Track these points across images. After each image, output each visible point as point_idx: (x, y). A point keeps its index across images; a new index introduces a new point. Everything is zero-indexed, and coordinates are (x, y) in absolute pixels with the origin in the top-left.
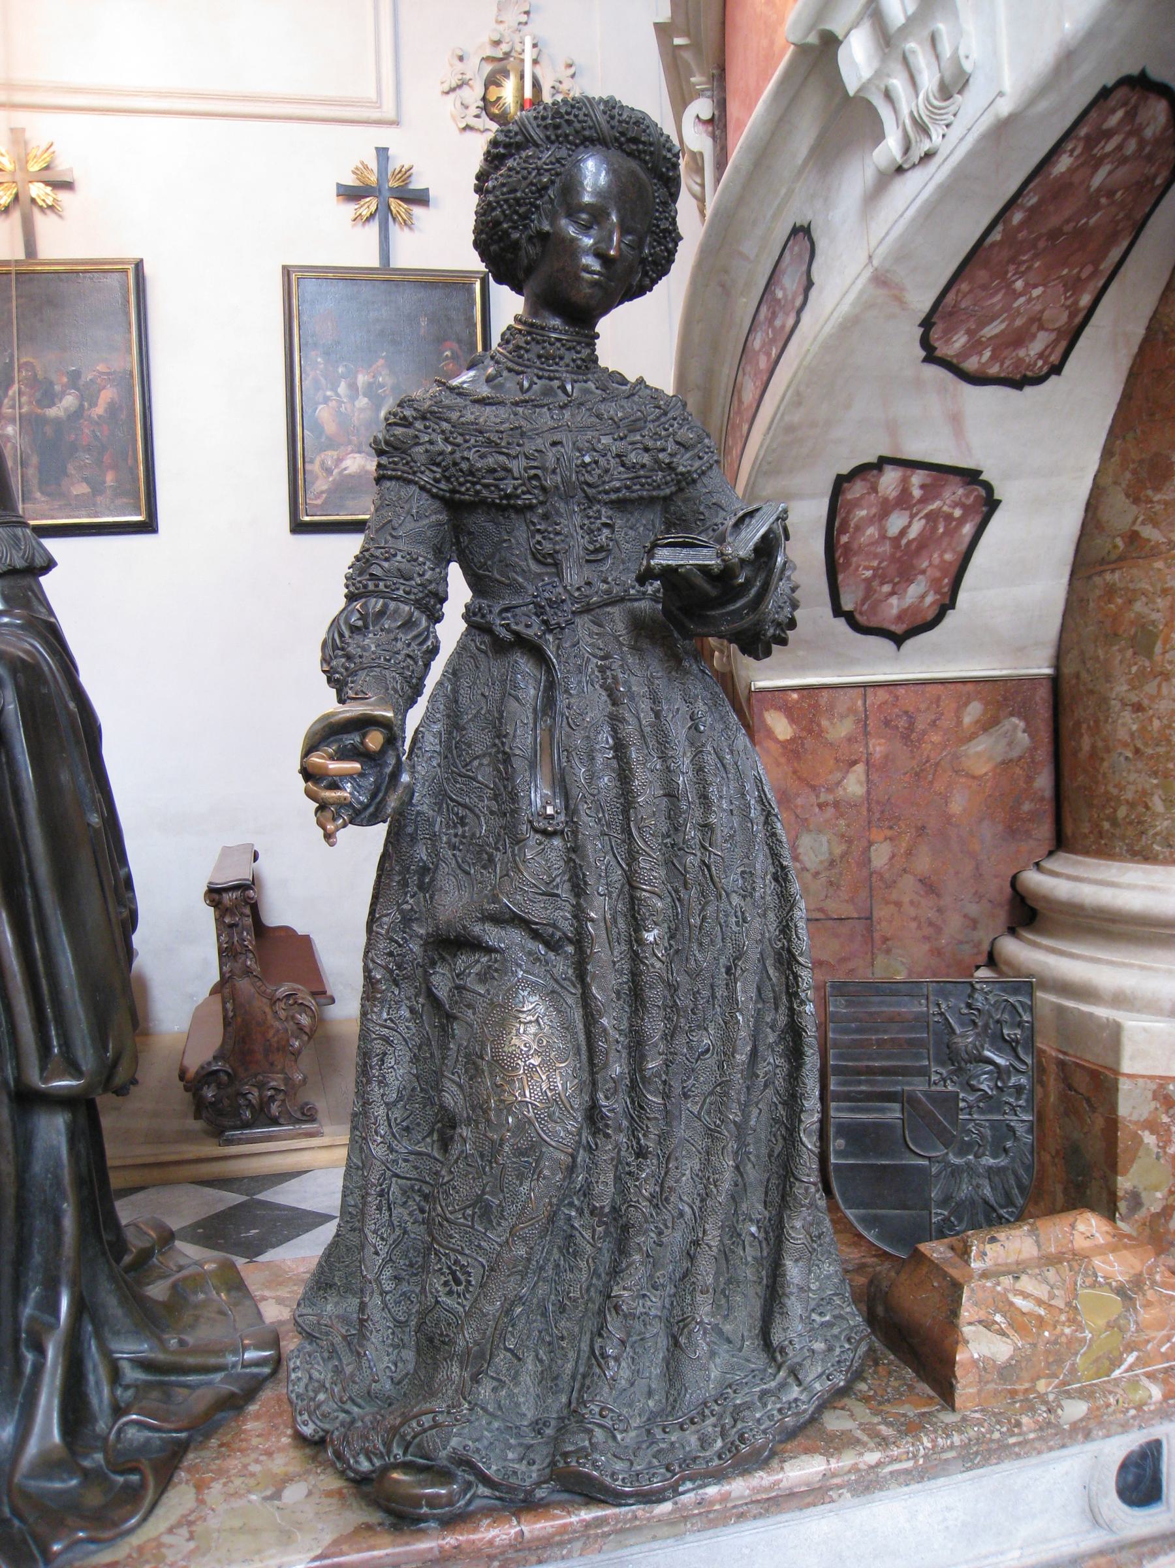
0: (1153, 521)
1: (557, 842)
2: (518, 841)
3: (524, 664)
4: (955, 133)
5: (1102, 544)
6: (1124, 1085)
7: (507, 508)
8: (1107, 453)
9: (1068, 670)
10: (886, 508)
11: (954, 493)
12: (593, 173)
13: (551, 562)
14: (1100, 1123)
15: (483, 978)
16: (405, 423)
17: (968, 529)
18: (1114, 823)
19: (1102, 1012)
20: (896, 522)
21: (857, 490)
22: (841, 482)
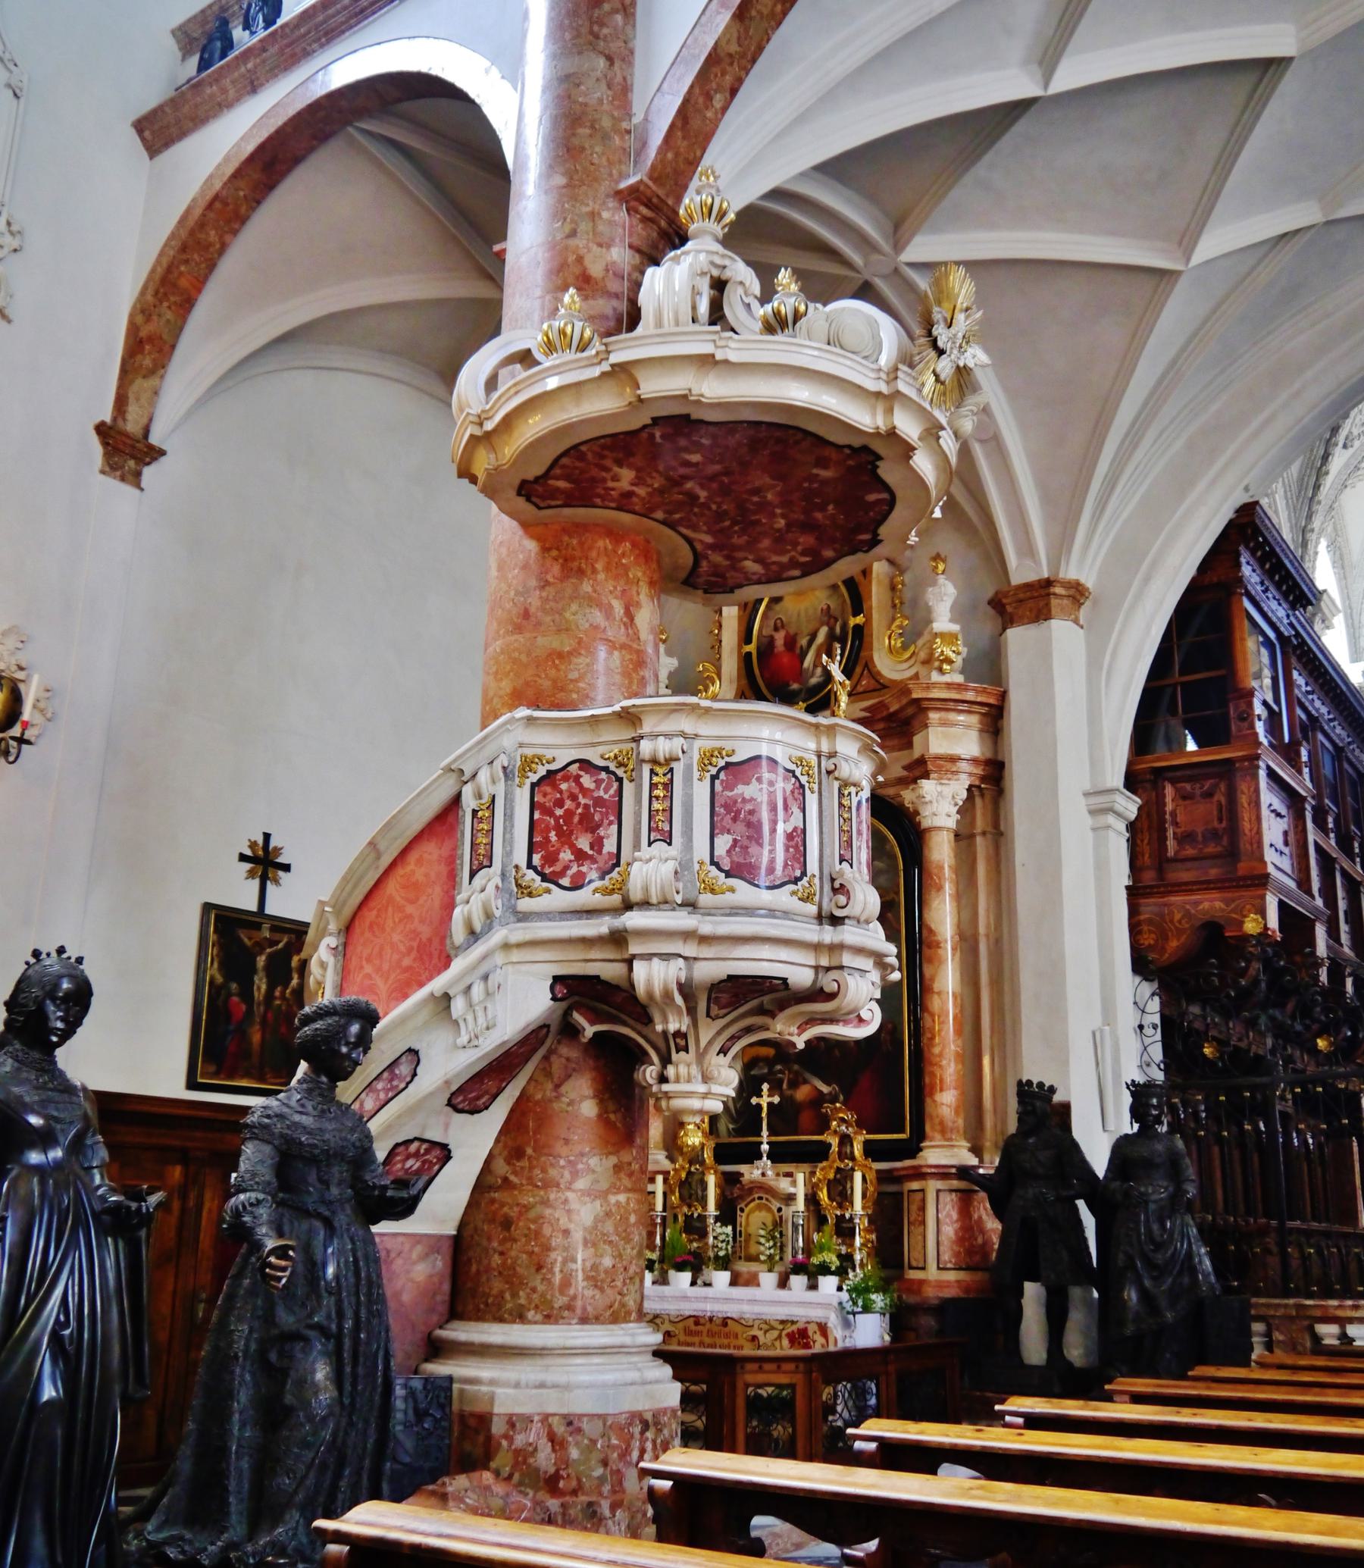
0: (515, 1173)
1: (333, 1298)
2: (319, 1297)
3: (318, 1224)
4: (488, 1042)
5: (490, 1180)
6: (495, 1419)
7: (313, 1161)
8: (497, 1141)
9: (466, 1234)
10: (408, 1157)
11: (437, 1152)
12: (355, 1028)
13: (326, 1184)
14: (481, 1439)
15: (303, 1350)
16: (268, 1117)
17: (436, 1167)
18: (487, 1305)
19: (484, 1389)
20: (409, 1163)
21: (401, 1149)
22: (397, 1145)
